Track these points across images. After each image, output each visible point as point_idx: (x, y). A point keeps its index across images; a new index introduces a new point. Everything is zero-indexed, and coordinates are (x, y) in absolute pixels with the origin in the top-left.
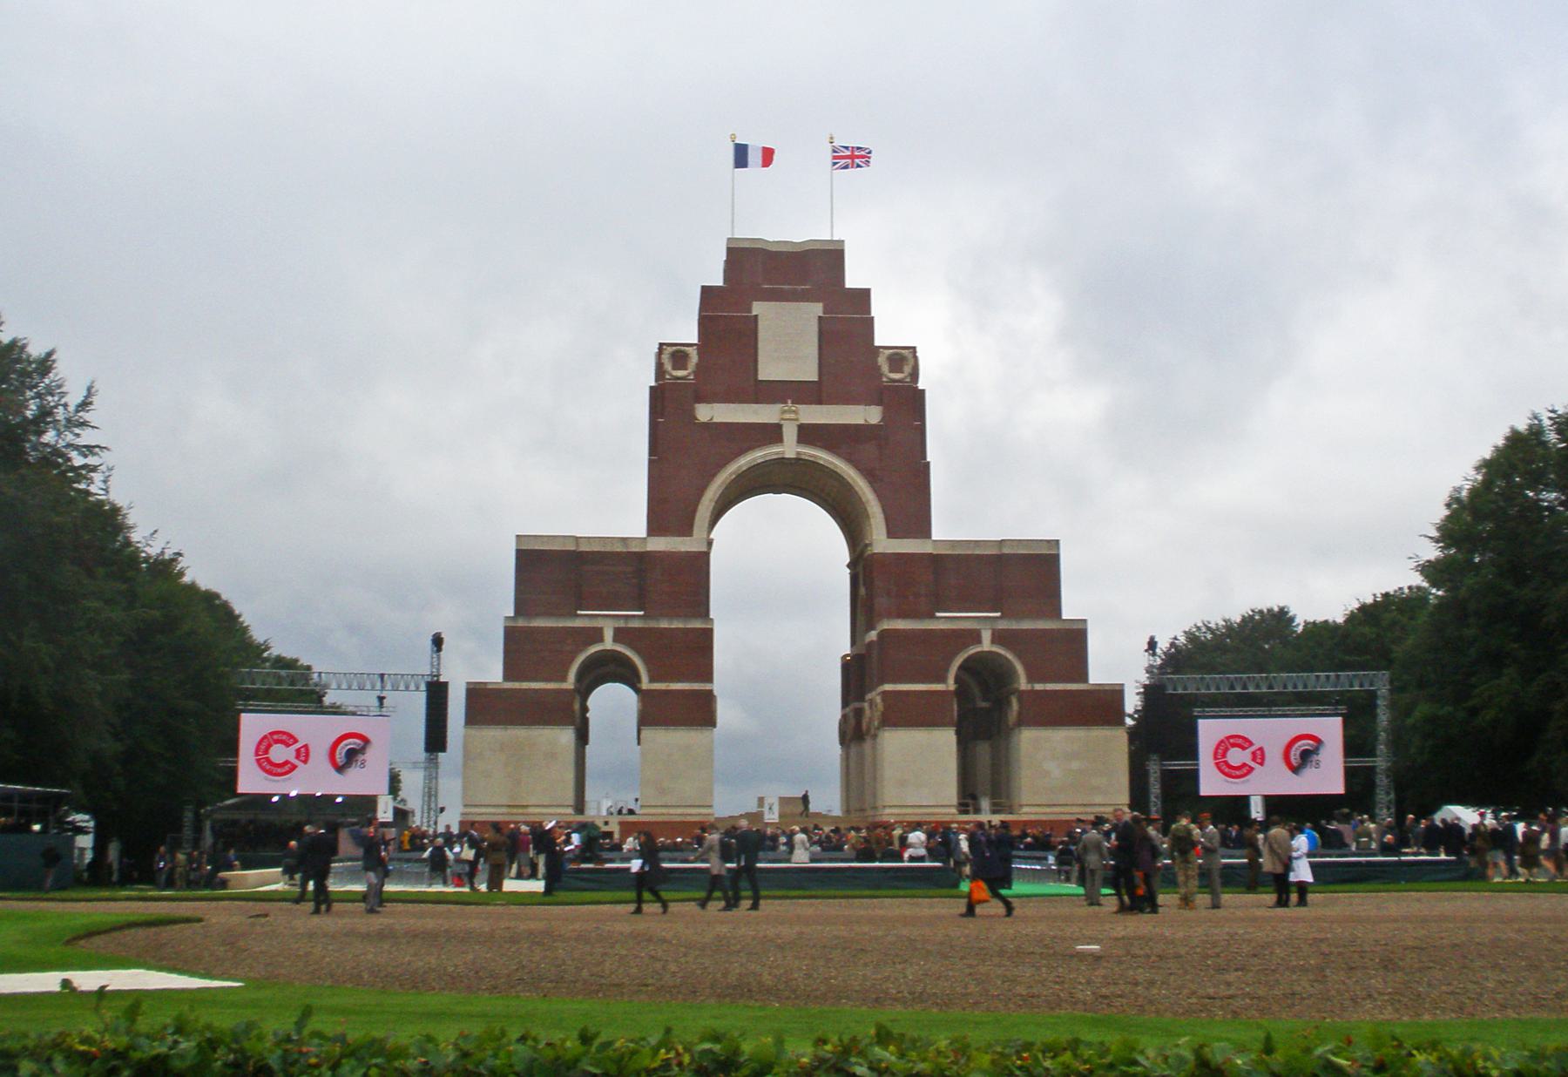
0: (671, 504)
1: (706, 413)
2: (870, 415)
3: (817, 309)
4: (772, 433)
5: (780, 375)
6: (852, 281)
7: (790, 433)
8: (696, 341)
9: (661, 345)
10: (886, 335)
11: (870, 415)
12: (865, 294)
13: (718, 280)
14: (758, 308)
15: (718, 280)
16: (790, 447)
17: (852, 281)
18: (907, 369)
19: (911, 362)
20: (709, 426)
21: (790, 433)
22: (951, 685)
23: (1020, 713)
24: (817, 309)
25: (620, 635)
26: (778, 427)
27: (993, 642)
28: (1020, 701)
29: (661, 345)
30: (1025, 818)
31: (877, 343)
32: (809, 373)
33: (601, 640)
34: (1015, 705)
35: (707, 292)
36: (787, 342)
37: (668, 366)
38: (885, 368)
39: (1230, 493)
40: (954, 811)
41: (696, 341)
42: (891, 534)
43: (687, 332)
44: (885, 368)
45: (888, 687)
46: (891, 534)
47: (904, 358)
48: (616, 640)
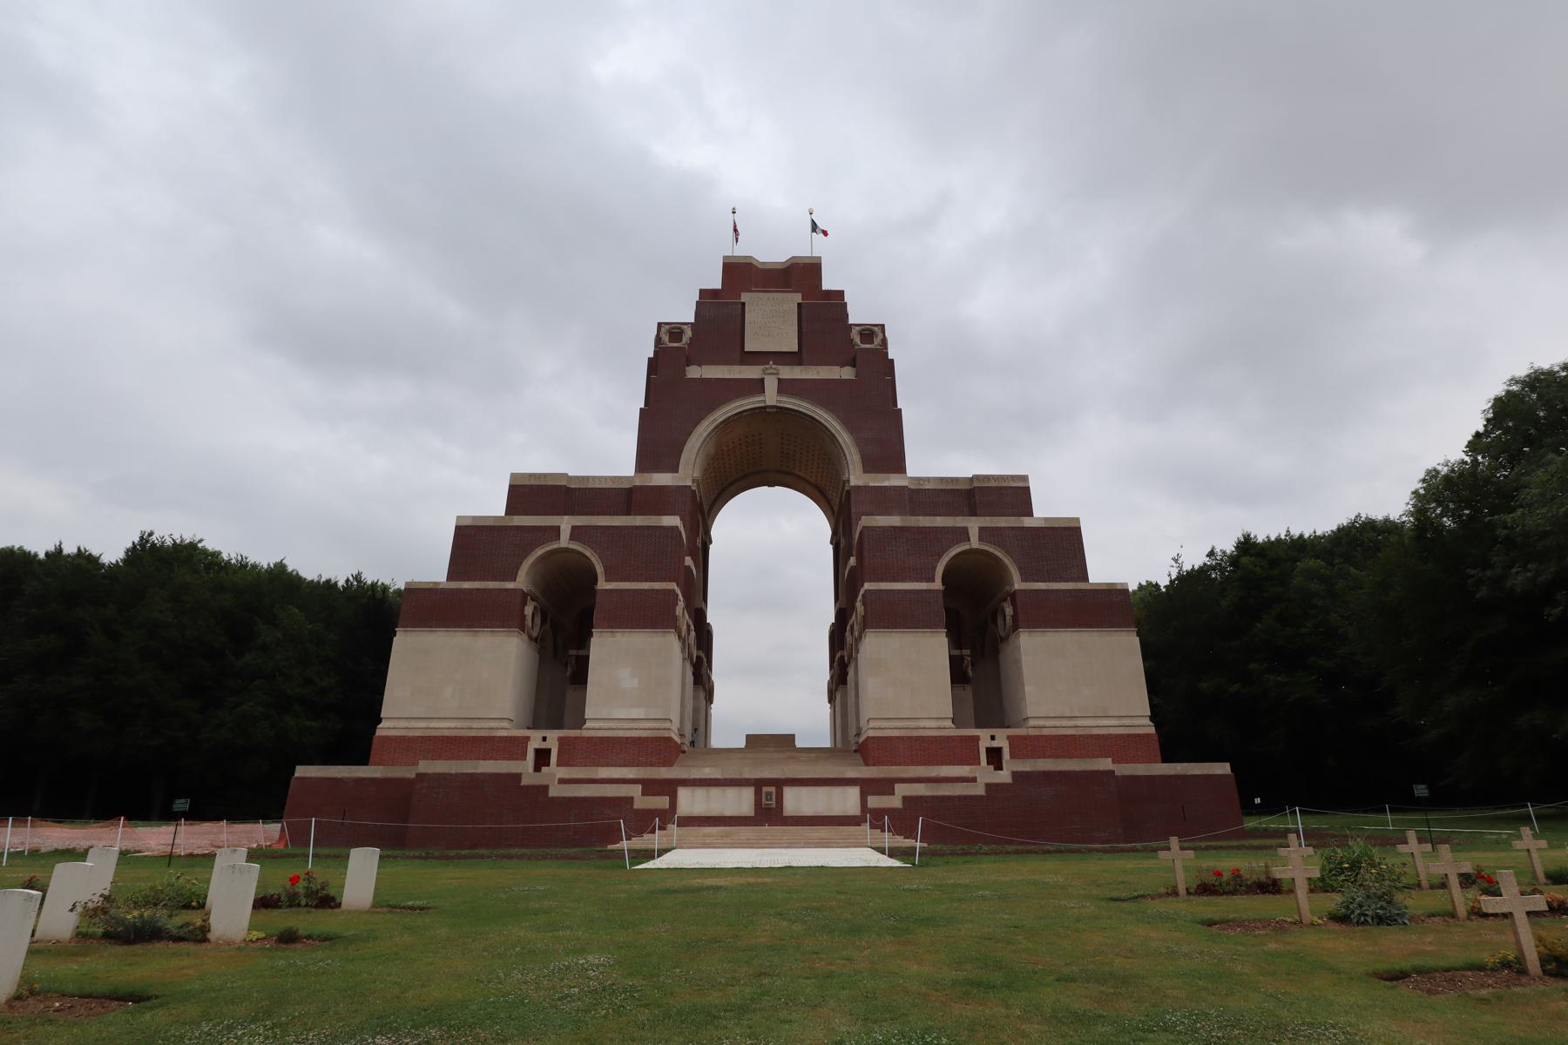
0: (656, 443)
1: (694, 372)
2: (847, 373)
3: (798, 298)
4: (758, 386)
5: (772, 376)
6: (826, 286)
7: (771, 385)
8: (692, 320)
9: (660, 325)
10: (858, 314)
11: (847, 373)
12: (841, 294)
13: (716, 284)
14: (745, 297)
15: (716, 284)
16: (771, 397)
17: (826, 286)
18: (877, 341)
19: (880, 336)
20: (701, 380)
21: (771, 385)
22: (937, 585)
23: (1015, 617)
24: (798, 298)
25: (576, 533)
26: (762, 380)
27: (981, 539)
28: (1014, 603)
29: (660, 325)
30: (1032, 732)
31: (851, 321)
32: (788, 342)
33: (558, 537)
34: (1009, 611)
35: (703, 292)
36: (771, 323)
37: (666, 338)
38: (857, 340)
39: (1182, 433)
40: (949, 723)
41: (692, 320)
42: (866, 471)
43: (686, 314)
44: (857, 340)
45: (867, 586)
46: (866, 471)
47: (872, 333)
48: (573, 537)
